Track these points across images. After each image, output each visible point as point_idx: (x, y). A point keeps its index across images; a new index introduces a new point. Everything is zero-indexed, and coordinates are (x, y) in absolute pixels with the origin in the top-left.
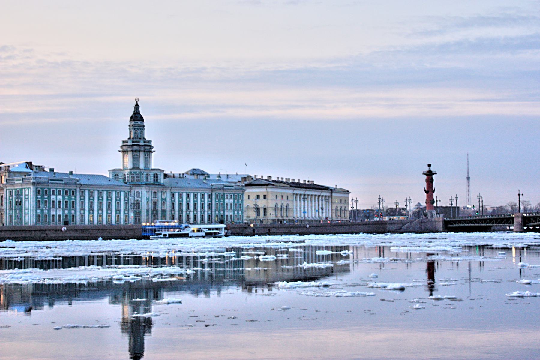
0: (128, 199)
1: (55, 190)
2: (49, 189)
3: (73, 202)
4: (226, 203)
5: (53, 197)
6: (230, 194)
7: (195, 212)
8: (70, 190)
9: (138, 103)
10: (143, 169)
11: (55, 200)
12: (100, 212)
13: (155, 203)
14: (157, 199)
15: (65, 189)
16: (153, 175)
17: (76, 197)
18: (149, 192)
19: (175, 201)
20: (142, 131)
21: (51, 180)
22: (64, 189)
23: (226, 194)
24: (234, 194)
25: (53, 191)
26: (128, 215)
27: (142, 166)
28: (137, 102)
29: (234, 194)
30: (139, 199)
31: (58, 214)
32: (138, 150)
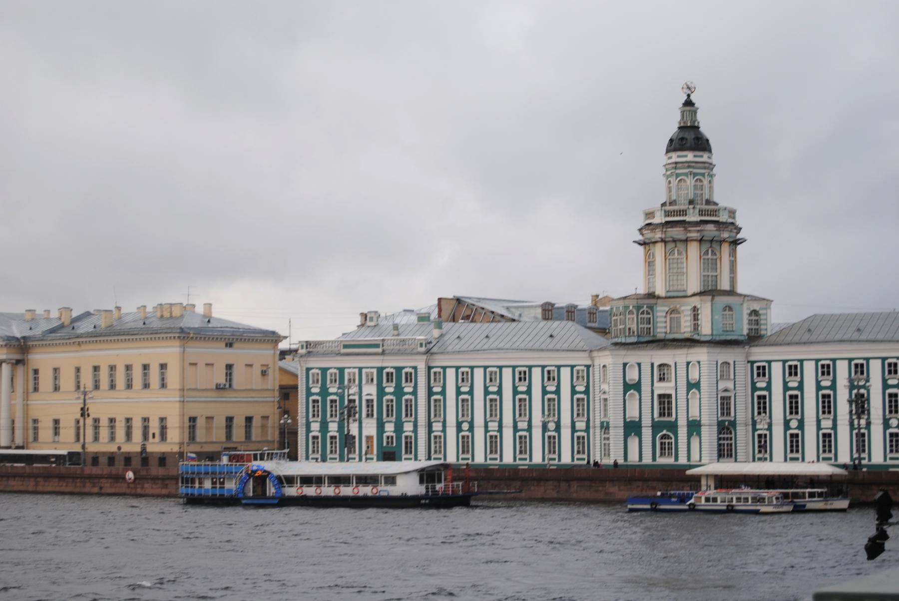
0: (587, 387)
1: (357, 371)
2: (341, 370)
8: (399, 369)
9: (693, 98)
10: (659, 297)
13: (665, 400)
16: (689, 313)
17: (415, 387)
18: (639, 365)
19: (768, 388)
20: (710, 182)
21: (345, 346)
22: (380, 370)
26: (585, 434)
27: (660, 291)
28: (689, 96)
30: (605, 387)
32: (683, 237)
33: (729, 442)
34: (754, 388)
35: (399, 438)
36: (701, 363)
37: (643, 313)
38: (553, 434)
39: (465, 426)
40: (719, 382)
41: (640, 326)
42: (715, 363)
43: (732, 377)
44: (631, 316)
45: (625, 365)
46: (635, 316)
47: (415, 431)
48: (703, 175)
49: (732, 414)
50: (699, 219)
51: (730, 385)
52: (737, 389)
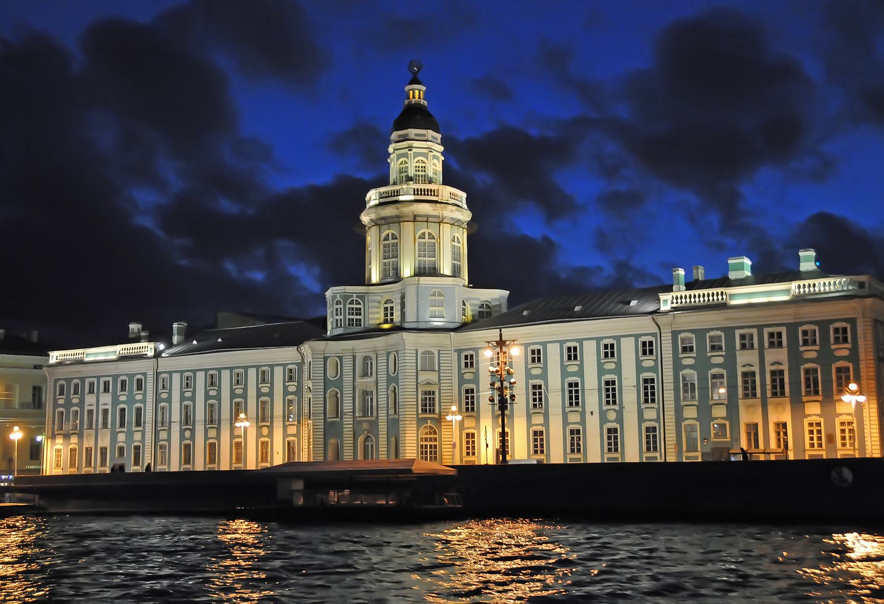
1: (95, 380)
3: (139, 410)
4: (740, 370)
5: (90, 399)
6: (766, 331)
7: (574, 418)
8: (131, 376)
11: (94, 408)
12: (212, 433)
14: (373, 379)
15: (119, 376)
17: (145, 395)
18: (340, 358)
23: (738, 333)
24: (792, 328)
25: (91, 385)
29: (792, 328)
31: (101, 444)
33: (433, 443)
34: (462, 380)
35: (129, 447)
36: (399, 352)
37: (350, 304)
38: (266, 439)
39: (188, 434)
40: (419, 372)
41: (348, 317)
42: (415, 352)
43: (437, 369)
44: (339, 306)
45: (325, 359)
46: (341, 306)
47: (143, 440)
48: (425, 155)
49: (437, 411)
50: (412, 198)
51: (433, 377)
52: (442, 381)
